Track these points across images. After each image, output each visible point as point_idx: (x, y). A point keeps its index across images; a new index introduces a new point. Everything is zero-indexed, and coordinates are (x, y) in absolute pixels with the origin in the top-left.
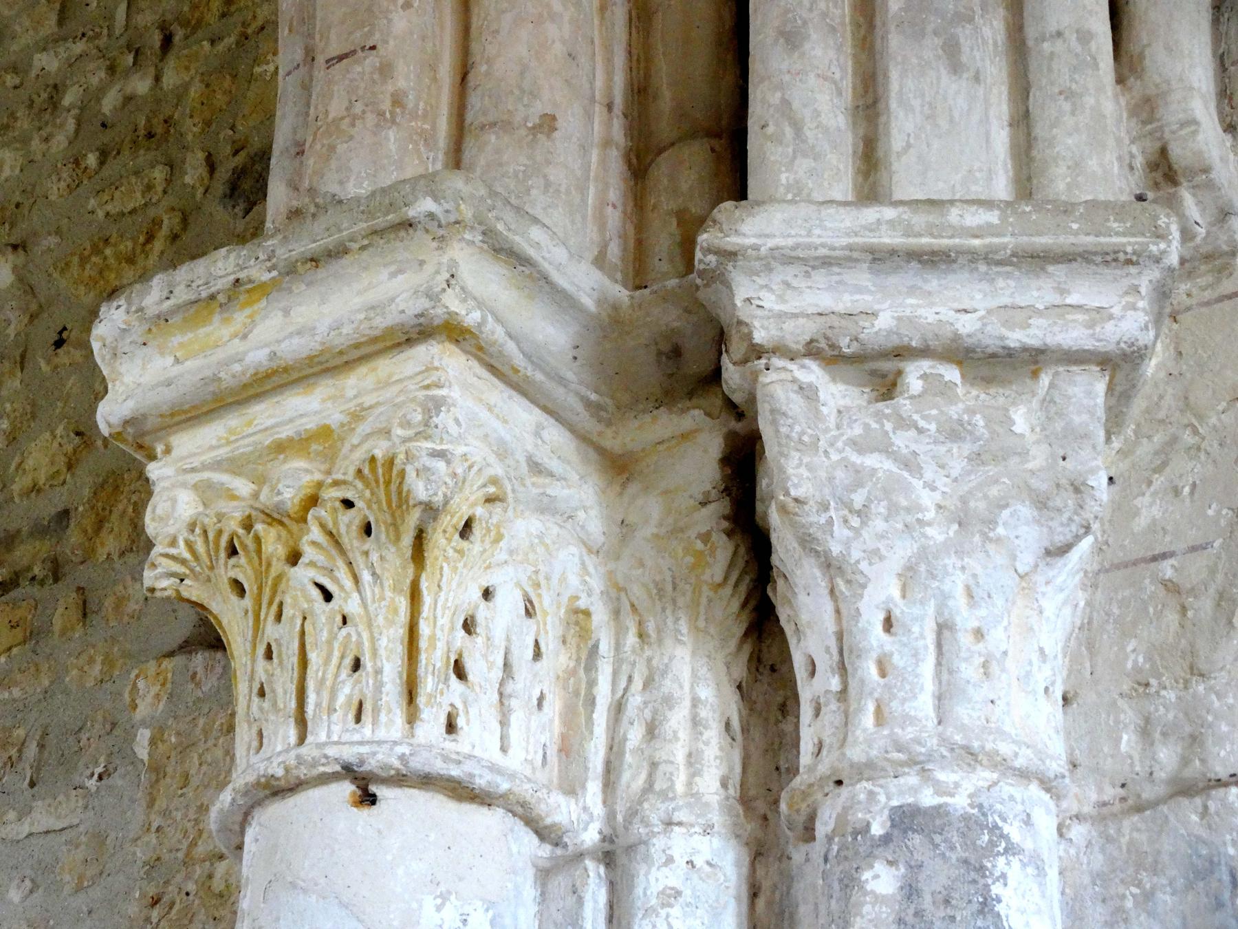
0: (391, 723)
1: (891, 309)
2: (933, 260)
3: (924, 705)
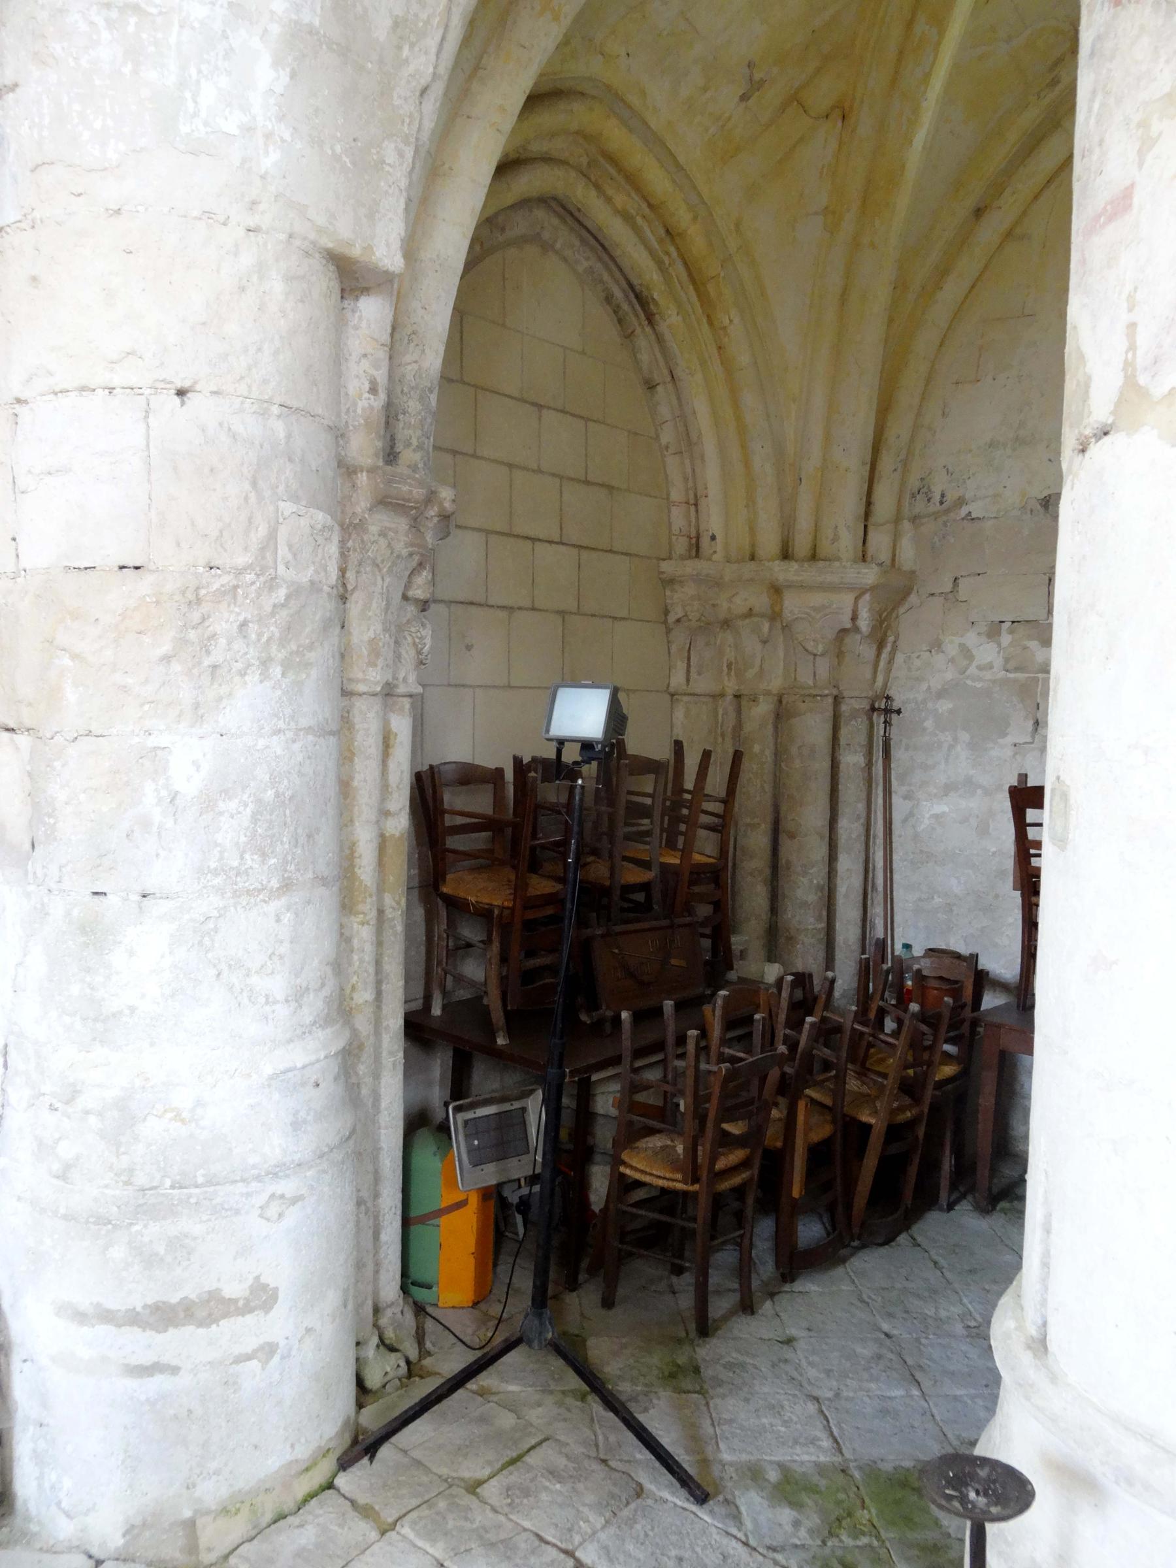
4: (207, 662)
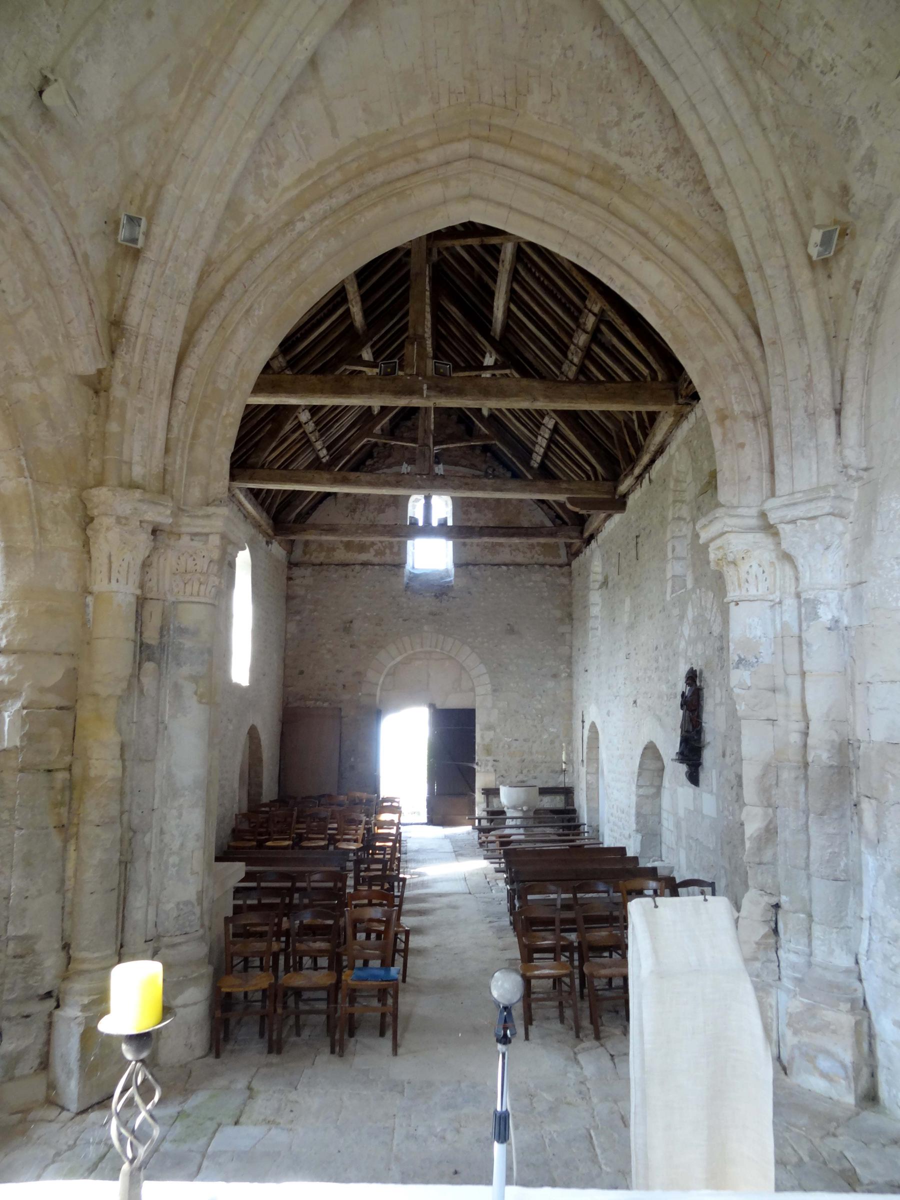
2: (794, 504)
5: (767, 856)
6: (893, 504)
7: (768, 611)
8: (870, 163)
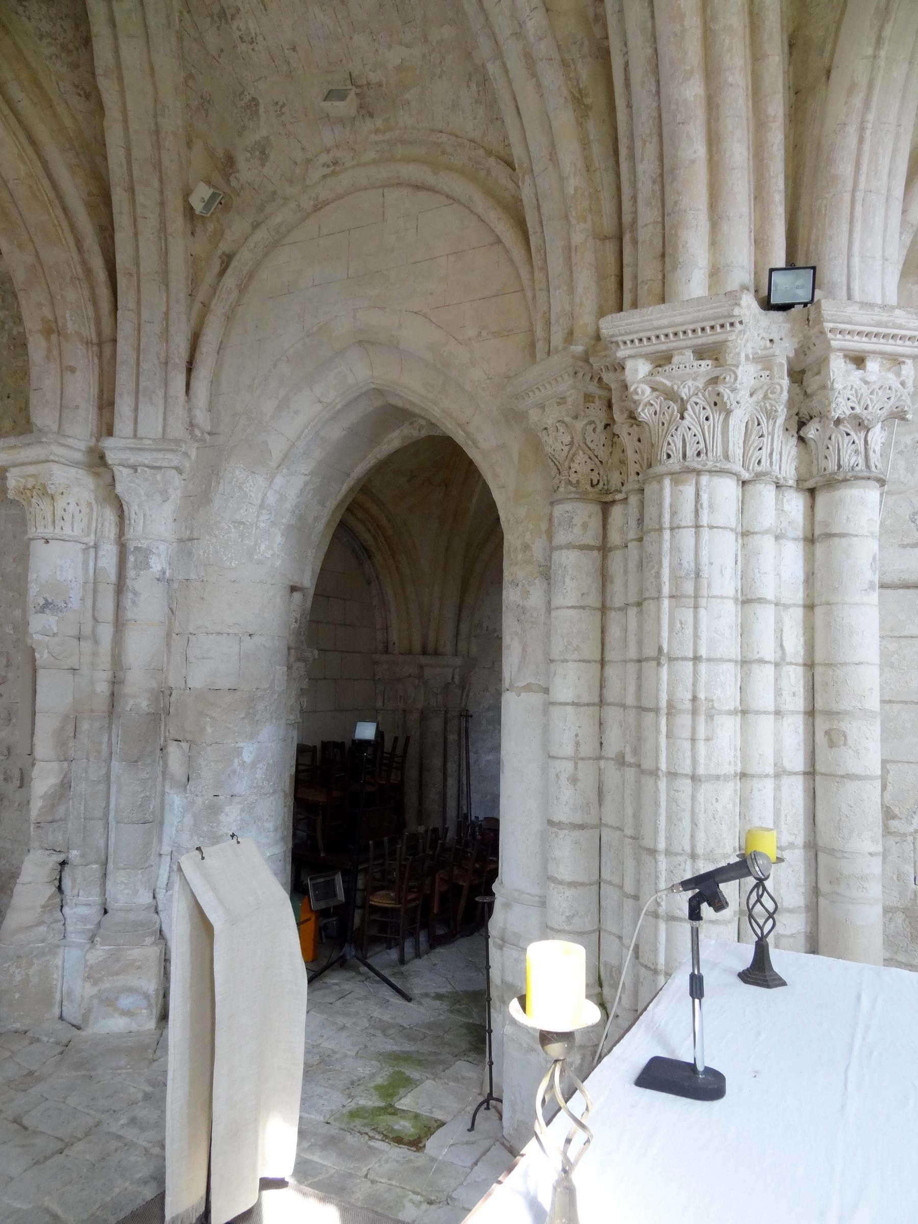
0: (50, 529)
1: (134, 458)
3: (140, 528)
4: (255, 719)
5: (61, 811)
6: (237, 472)
7: (80, 554)
8: (262, 151)
